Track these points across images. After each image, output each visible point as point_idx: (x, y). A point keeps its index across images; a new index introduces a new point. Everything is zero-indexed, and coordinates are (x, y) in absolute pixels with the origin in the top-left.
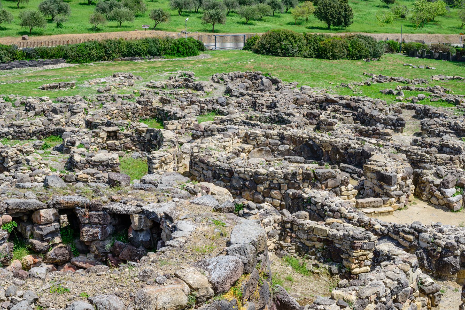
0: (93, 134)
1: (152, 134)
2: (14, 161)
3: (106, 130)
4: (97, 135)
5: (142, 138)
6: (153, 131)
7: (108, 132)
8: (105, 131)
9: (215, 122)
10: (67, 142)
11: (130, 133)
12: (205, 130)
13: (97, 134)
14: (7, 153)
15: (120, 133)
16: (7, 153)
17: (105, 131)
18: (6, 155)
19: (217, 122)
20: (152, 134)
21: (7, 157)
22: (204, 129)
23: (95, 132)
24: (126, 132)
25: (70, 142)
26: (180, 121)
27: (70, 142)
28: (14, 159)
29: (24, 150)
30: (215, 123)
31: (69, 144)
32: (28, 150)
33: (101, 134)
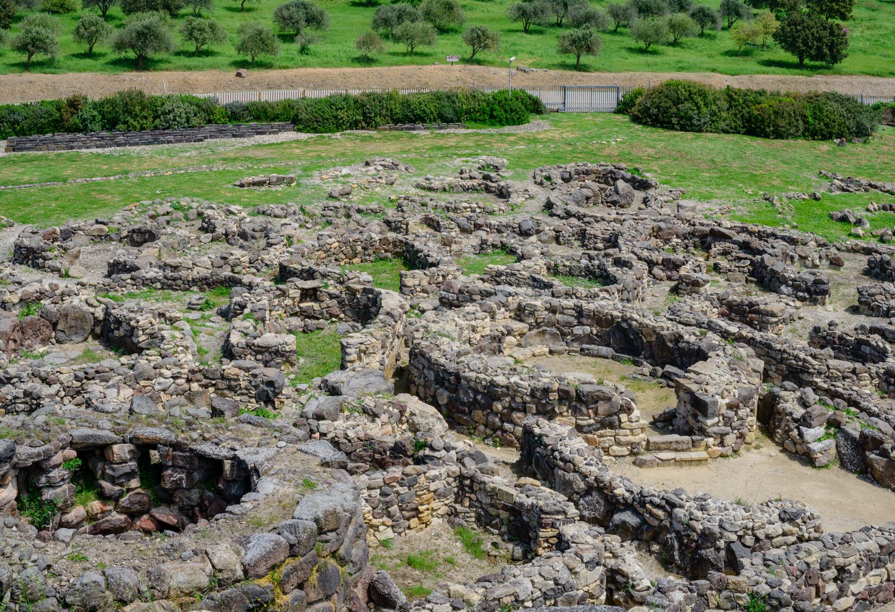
0: (278, 292)
1: (370, 296)
2: (147, 334)
3: (300, 286)
4: (284, 294)
5: (355, 301)
6: (371, 291)
7: (302, 289)
8: (298, 288)
9: (482, 276)
10: (235, 304)
11: (337, 292)
12: (461, 292)
13: (285, 293)
14: (138, 322)
15: (321, 292)
16: (138, 322)
17: (298, 288)
18: (135, 325)
19: (486, 277)
20: (370, 296)
21: (137, 327)
22: (460, 290)
23: (280, 290)
24: (331, 290)
25: (239, 305)
26: (427, 272)
27: (239, 305)
28: (147, 331)
29: (168, 315)
30: (482, 279)
31: (237, 307)
32: (174, 315)
33: (291, 291)
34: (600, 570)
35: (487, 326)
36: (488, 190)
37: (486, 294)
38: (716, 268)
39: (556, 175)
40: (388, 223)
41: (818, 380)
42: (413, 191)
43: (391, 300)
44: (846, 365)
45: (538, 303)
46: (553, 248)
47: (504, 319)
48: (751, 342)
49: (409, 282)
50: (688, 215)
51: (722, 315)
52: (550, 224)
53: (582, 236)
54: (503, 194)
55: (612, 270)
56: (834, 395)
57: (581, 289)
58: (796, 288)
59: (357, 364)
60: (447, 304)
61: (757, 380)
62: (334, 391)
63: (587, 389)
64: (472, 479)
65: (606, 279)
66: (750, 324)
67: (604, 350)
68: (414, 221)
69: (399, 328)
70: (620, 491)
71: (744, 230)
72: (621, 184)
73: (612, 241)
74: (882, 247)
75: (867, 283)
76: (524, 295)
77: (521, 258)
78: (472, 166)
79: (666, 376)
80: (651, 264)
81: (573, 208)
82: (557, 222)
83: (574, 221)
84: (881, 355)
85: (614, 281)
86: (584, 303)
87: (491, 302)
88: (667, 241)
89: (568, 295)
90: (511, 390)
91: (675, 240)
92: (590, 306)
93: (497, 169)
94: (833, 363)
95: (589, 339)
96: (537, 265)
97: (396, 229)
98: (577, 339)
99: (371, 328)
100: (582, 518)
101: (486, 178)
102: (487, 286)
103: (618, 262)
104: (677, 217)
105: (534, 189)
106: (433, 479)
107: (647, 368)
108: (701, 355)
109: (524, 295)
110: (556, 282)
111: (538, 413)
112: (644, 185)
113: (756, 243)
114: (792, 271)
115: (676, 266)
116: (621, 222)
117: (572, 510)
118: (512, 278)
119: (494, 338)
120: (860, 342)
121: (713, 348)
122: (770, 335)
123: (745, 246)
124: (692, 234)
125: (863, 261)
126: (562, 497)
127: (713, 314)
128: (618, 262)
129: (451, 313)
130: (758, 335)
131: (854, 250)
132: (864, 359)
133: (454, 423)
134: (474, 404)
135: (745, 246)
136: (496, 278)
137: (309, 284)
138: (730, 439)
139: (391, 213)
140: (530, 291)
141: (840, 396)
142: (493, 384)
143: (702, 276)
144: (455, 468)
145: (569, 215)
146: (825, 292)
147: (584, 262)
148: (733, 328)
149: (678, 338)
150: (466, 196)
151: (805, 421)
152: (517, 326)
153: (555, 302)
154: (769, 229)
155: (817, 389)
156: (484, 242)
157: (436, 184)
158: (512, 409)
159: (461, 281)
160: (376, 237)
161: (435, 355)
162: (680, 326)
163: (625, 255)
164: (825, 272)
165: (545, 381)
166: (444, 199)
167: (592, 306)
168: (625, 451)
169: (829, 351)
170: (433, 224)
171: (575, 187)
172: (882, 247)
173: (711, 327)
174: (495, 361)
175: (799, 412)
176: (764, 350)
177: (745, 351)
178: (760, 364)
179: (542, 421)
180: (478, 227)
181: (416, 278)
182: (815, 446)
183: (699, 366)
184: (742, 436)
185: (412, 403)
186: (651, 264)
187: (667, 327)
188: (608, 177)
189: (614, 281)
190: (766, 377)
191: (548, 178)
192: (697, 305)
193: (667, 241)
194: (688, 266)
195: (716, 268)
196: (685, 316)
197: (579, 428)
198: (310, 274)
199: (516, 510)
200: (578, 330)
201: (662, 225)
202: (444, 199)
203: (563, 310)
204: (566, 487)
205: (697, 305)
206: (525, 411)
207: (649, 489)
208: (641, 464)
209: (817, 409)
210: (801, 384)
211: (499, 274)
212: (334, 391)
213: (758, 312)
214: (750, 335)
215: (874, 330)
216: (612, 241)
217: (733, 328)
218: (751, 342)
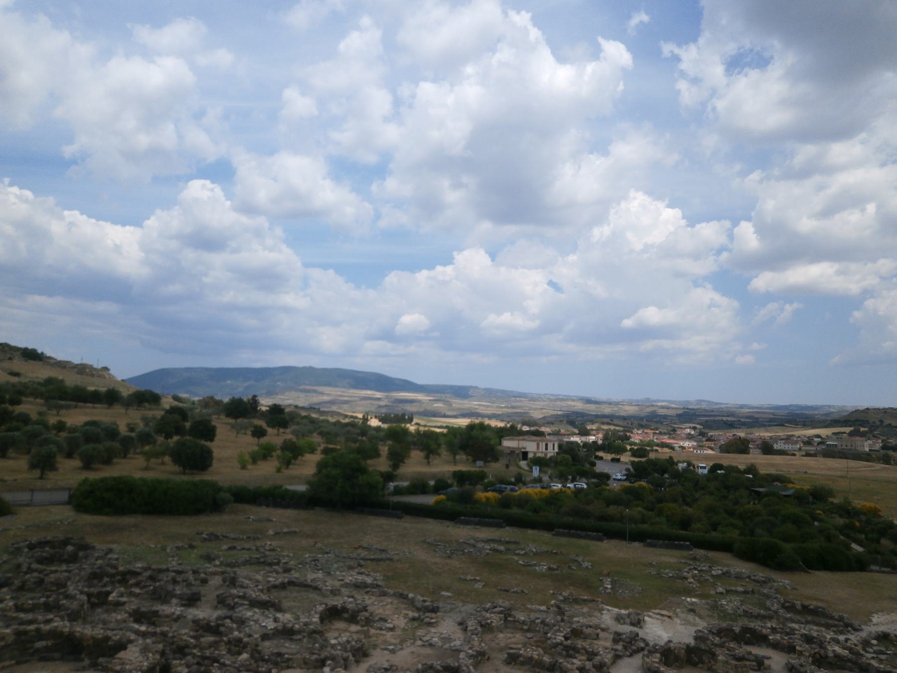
41: (195, 651)
48: (154, 634)
57: (40, 618)
66: (153, 624)
67: (57, 655)
86: (42, 626)
89: (31, 622)
91: (106, 579)
95: (47, 649)
98: (38, 650)
104: (108, 565)
107: (87, 662)
110: (22, 615)
116: (69, 571)
120: (218, 626)
121: (130, 642)
146: (199, 599)
147: (43, 600)
148: (143, 628)
153: (22, 628)
154: (164, 567)
162: (108, 632)
167: (48, 627)
171: (38, 552)
183: (122, 654)
194: (114, 594)
201: (98, 571)
214: (153, 631)
217: (143, 628)
218: (154, 634)
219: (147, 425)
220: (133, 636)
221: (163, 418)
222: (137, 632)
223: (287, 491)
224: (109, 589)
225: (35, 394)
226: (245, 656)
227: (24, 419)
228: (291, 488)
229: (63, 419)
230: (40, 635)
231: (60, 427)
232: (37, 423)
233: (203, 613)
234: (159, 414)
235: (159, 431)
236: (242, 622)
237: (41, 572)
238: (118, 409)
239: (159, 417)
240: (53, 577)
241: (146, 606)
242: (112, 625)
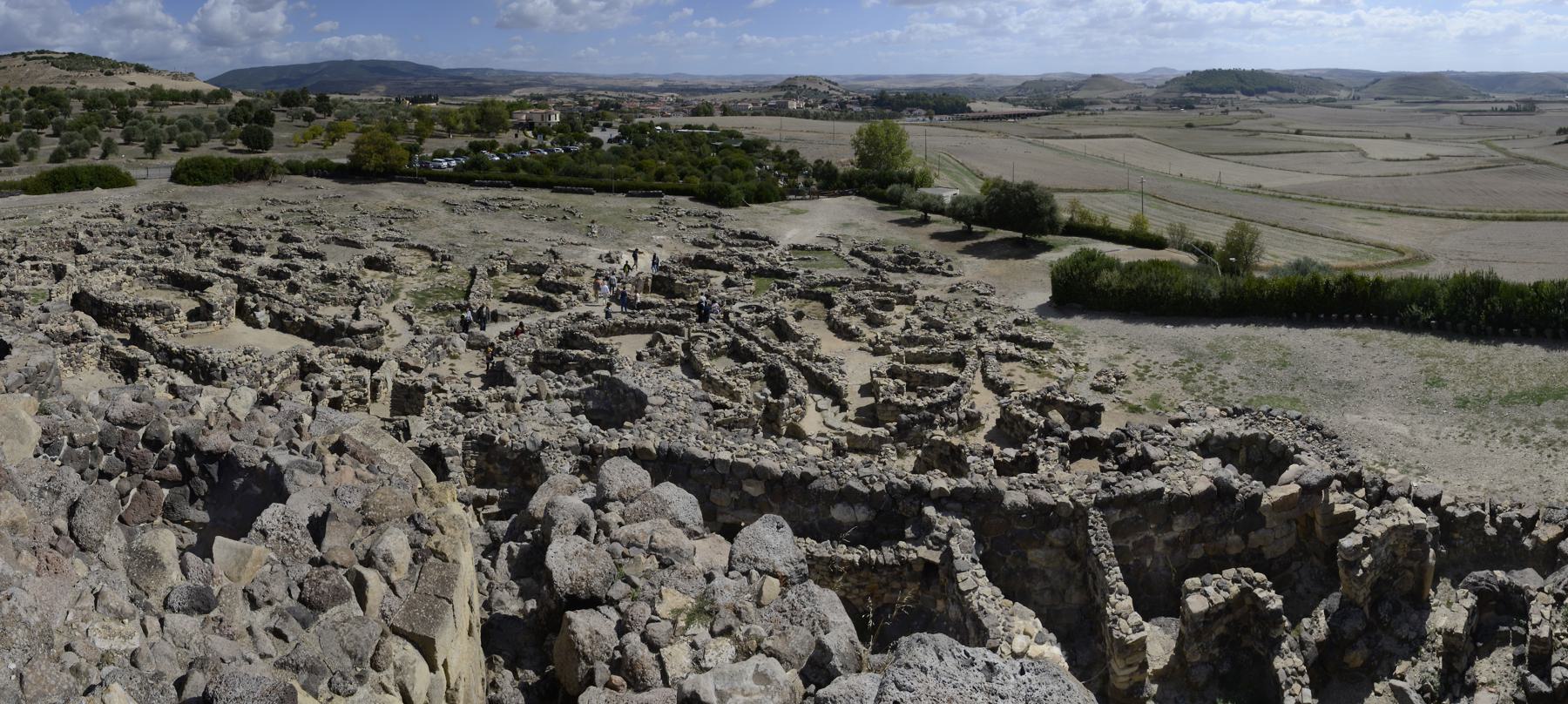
34: (165, 384)
35: (114, 278)
36: (114, 216)
37: (113, 264)
38: (217, 245)
39: (144, 207)
40: (69, 234)
42: (80, 219)
43: (71, 268)
44: (274, 282)
45: (137, 266)
46: (144, 241)
47: (122, 274)
48: (232, 276)
49: (79, 260)
50: (204, 222)
51: (219, 265)
52: (142, 231)
53: (157, 235)
54: (121, 218)
55: (171, 249)
56: (268, 296)
58: (252, 250)
59: (56, 299)
60: (94, 269)
61: (234, 293)
62: (46, 310)
63: (159, 304)
64: (108, 348)
65: (166, 253)
66: (232, 268)
68: (82, 235)
69: (75, 281)
70: (174, 349)
71: (228, 226)
72: (174, 210)
73: (170, 236)
74: (288, 228)
75: (281, 244)
76: (131, 263)
77: (129, 247)
78: (107, 206)
79: (195, 295)
80: (187, 245)
81: (152, 222)
82: (145, 229)
83: (153, 228)
84: (288, 276)
85: (171, 254)
87: (115, 267)
88: (195, 234)
89: (151, 262)
90: (126, 307)
92: (160, 266)
93: (118, 206)
94: (267, 282)
95: (161, 281)
96: (137, 250)
97: (73, 237)
99: (62, 282)
100: (157, 362)
101: (113, 211)
102: (114, 260)
103: (174, 246)
105: (134, 215)
106: (91, 348)
108: (210, 284)
109: (131, 263)
111: (138, 316)
112: (183, 209)
113: (234, 232)
114: (251, 242)
115: (198, 245)
117: (152, 358)
118: (125, 256)
119: (117, 283)
121: (215, 280)
122: (240, 272)
123: (229, 234)
124: (206, 230)
125: (280, 235)
126: (148, 353)
127: (216, 266)
128: (174, 246)
129: (97, 273)
130: (235, 273)
131: (276, 231)
132: (281, 278)
133: (101, 324)
134: (109, 315)
135: (229, 234)
136: (118, 256)
137: (34, 263)
138: (224, 321)
139: (71, 230)
140: (133, 261)
141: (271, 296)
142: (117, 304)
143: (212, 248)
144: (100, 344)
145: (150, 225)
146: (264, 251)
148: (224, 271)
149: (200, 277)
150: (104, 220)
151: (256, 309)
152: (128, 278)
153: (145, 265)
155: (261, 294)
156: (112, 240)
157: (90, 215)
158: (126, 316)
159: (102, 258)
160: (64, 241)
161: (91, 293)
163: (176, 242)
164: (264, 241)
165: (141, 301)
166: (94, 221)
168: (177, 330)
169: (266, 276)
170: (90, 233)
171: (153, 213)
172: (288, 228)
173: (214, 271)
174: (119, 294)
175: (253, 305)
176: (237, 279)
177: (229, 281)
178: (236, 286)
179: (140, 320)
180: (110, 233)
181: (82, 258)
182: (261, 320)
183: (208, 289)
184: (229, 319)
185: (81, 315)
186: (187, 245)
187: (193, 272)
188: (168, 207)
189: (171, 254)
190: (239, 291)
191: (141, 209)
192: (208, 262)
193: (195, 234)
194: (205, 244)
195: (217, 245)
196: (202, 268)
197: (156, 322)
198: (34, 258)
199: (127, 360)
200: (156, 278)
202: (94, 221)
203: (148, 269)
204: (150, 349)
205: (208, 262)
206: (132, 316)
207: (187, 347)
208: (184, 336)
209: (260, 303)
210: (254, 293)
211: (119, 254)
212: (46, 310)
213: (235, 262)
215: (285, 265)
216: (170, 236)
217: (224, 271)
218: (232, 276)
219: (221, 116)
220: (217, 276)
221: (233, 110)
222: (220, 274)
223: (332, 163)
224: (201, 241)
225: (143, 97)
226: (298, 296)
227: (138, 116)
228: (335, 161)
229: (164, 114)
230: (155, 270)
231: (163, 121)
232: (147, 119)
233: (266, 260)
234: (230, 105)
235: (231, 120)
236: (297, 268)
237: (156, 226)
238: (200, 104)
239: (230, 109)
240: (164, 231)
241: (227, 254)
242: (205, 268)
